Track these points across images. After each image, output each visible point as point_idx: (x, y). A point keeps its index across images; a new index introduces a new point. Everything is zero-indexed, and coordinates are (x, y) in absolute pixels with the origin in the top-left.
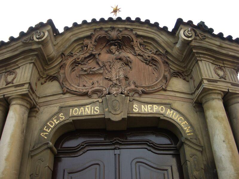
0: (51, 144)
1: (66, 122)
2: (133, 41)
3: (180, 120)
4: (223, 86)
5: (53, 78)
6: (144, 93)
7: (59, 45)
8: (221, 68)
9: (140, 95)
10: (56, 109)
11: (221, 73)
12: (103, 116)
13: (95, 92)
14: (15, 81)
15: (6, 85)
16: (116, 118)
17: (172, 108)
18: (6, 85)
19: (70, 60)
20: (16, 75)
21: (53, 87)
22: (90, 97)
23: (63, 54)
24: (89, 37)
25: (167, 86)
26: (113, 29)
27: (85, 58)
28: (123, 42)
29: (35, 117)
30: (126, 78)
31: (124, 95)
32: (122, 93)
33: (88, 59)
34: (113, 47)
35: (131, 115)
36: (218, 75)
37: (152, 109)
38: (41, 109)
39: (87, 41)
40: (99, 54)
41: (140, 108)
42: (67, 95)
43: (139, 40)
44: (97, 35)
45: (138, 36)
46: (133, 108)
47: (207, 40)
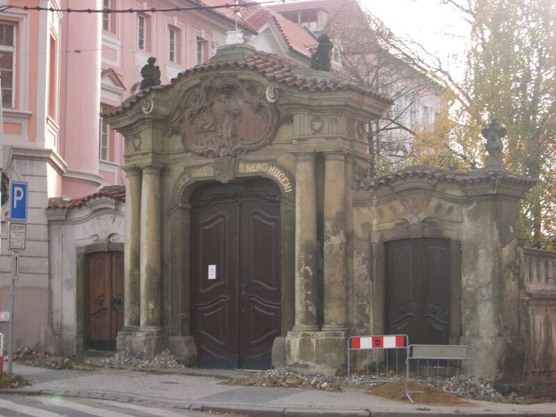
0: (180, 204)
1: (191, 183)
2: (239, 87)
3: (281, 177)
4: (314, 144)
5: (176, 132)
6: (248, 151)
7: (172, 98)
8: (318, 119)
9: (247, 153)
10: (182, 169)
11: (317, 125)
12: (214, 178)
13: (209, 152)
14: (141, 147)
15: (136, 150)
16: (225, 180)
17: (273, 165)
18: (136, 150)
19: (187, 114)
20: (141, 140)
21: (176, 143)
22: (207, 157)
23: (178, 108)
24: (197, 86)
25: (271, 141)
26: (216, 77)
27: (200, 110)
28: (230, 90)
29: (168, 175)
30: (234, 135)
31: (230, 157)
32: (228, 155)
33: (202, 111)
34: (223, 96)
35: (237, 176)
36: (313, 129)
37: (255, 168)
38: (173, 167)
39: (197, 90)
40: (212, 104)
41: (245, 168)
42: (189, 155)
43: (246, 85)
44: (205, 84)
45: (242, 81)
46: (239, 168)
47: (294, 95)
